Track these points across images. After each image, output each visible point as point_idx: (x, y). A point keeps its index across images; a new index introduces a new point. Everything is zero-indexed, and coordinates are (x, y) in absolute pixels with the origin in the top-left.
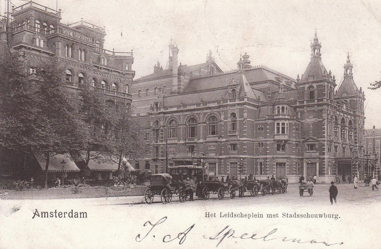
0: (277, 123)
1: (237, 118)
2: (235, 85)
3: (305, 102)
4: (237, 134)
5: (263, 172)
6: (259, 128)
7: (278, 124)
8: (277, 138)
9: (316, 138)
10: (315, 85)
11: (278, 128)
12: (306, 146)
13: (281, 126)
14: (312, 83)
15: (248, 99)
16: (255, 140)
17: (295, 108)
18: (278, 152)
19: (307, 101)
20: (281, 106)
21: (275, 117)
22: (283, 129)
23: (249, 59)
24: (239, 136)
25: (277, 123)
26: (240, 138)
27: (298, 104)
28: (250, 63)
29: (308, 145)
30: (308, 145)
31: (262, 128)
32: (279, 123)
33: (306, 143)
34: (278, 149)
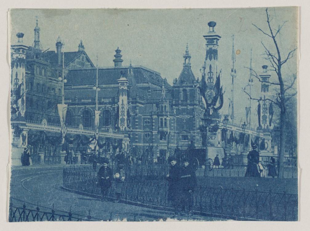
0: (161, 119)
3: (180, 101)
6: (146, 122)
10: (188, 89)
11: (162, 123)
12: (181, 137)
13: (164, 121)
18: (161, 141)
22: (166, 123)
23: (121, 53)
25: (161, 119)
28: (121, 57)
29: (182, 136)
30: (182, 136)
32: (162, 119)
33: (180, 134)
34: (161, 139)
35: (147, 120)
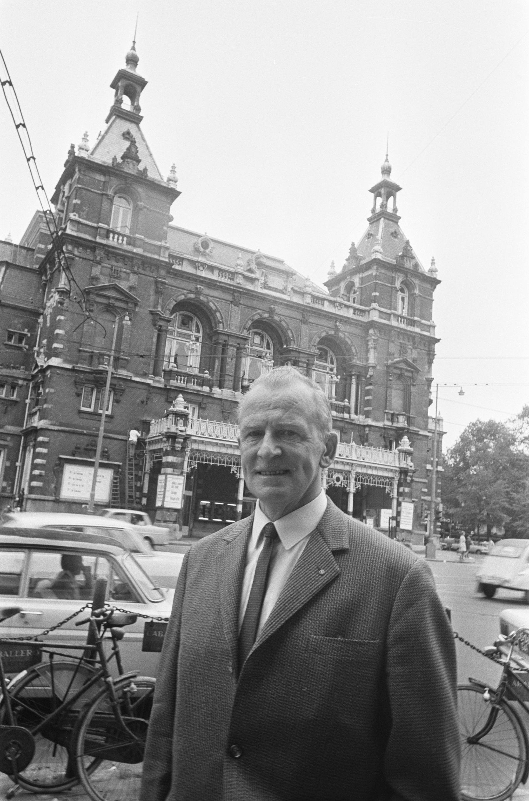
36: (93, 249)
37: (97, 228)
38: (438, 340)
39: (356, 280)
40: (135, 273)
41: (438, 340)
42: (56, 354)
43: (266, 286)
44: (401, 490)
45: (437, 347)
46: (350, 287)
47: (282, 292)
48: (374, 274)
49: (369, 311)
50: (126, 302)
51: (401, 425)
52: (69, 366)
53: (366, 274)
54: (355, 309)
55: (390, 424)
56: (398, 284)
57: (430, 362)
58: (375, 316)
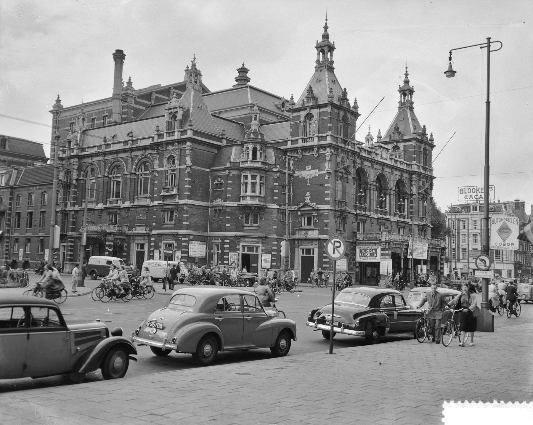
1: (176, 165)
2: (176, 108)
4: (175, 192)
5: (220, 262)
7: (246, 177)
8: (243, 202)
9: (315, 204)
14: (311, 109)
15: (195, 132)
16: (210, 204)
17: (285, 152)
19: (302, 139)
20: (251, 146)
21: (241, 165)
24: (177, 196)
26: (179, 199)
27: (289, 145)
31: (221, 184)
35: (219, 180)
36: (338, 149)
37: (337, 138)
38: (435, 178)
39: (401, 145)
40: (349, 159)
41: (435, 178)
42: (327, 203)
43: (382, 158)
44: (442, 257)
45: (434, 181)
46: (396, 148)
47: (386, 159)
48: (414, 145)
49: (411, 165)
50: (347, 175)
51: (424, 223)
52: (333, 209)
53: (407, 144)
54: (407, 164)
55: (420, 223)
56: (422, 150)
57: (432, 189)
58: (415, 168)
